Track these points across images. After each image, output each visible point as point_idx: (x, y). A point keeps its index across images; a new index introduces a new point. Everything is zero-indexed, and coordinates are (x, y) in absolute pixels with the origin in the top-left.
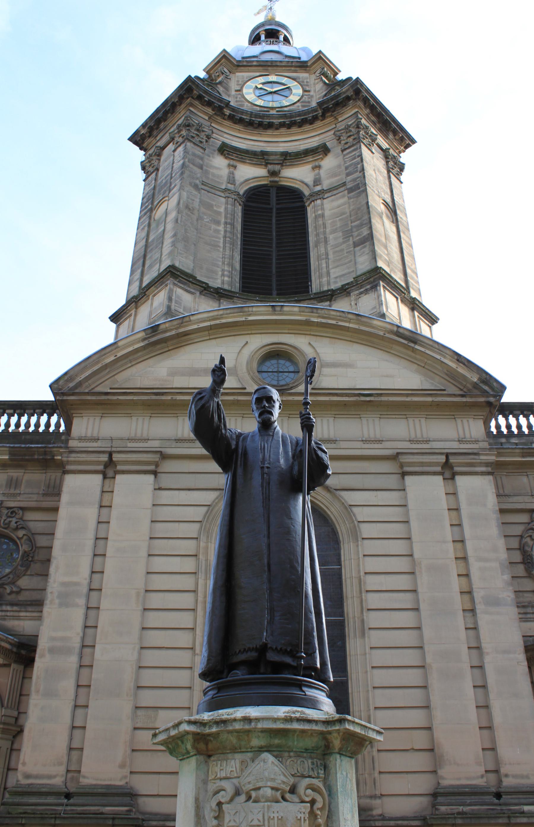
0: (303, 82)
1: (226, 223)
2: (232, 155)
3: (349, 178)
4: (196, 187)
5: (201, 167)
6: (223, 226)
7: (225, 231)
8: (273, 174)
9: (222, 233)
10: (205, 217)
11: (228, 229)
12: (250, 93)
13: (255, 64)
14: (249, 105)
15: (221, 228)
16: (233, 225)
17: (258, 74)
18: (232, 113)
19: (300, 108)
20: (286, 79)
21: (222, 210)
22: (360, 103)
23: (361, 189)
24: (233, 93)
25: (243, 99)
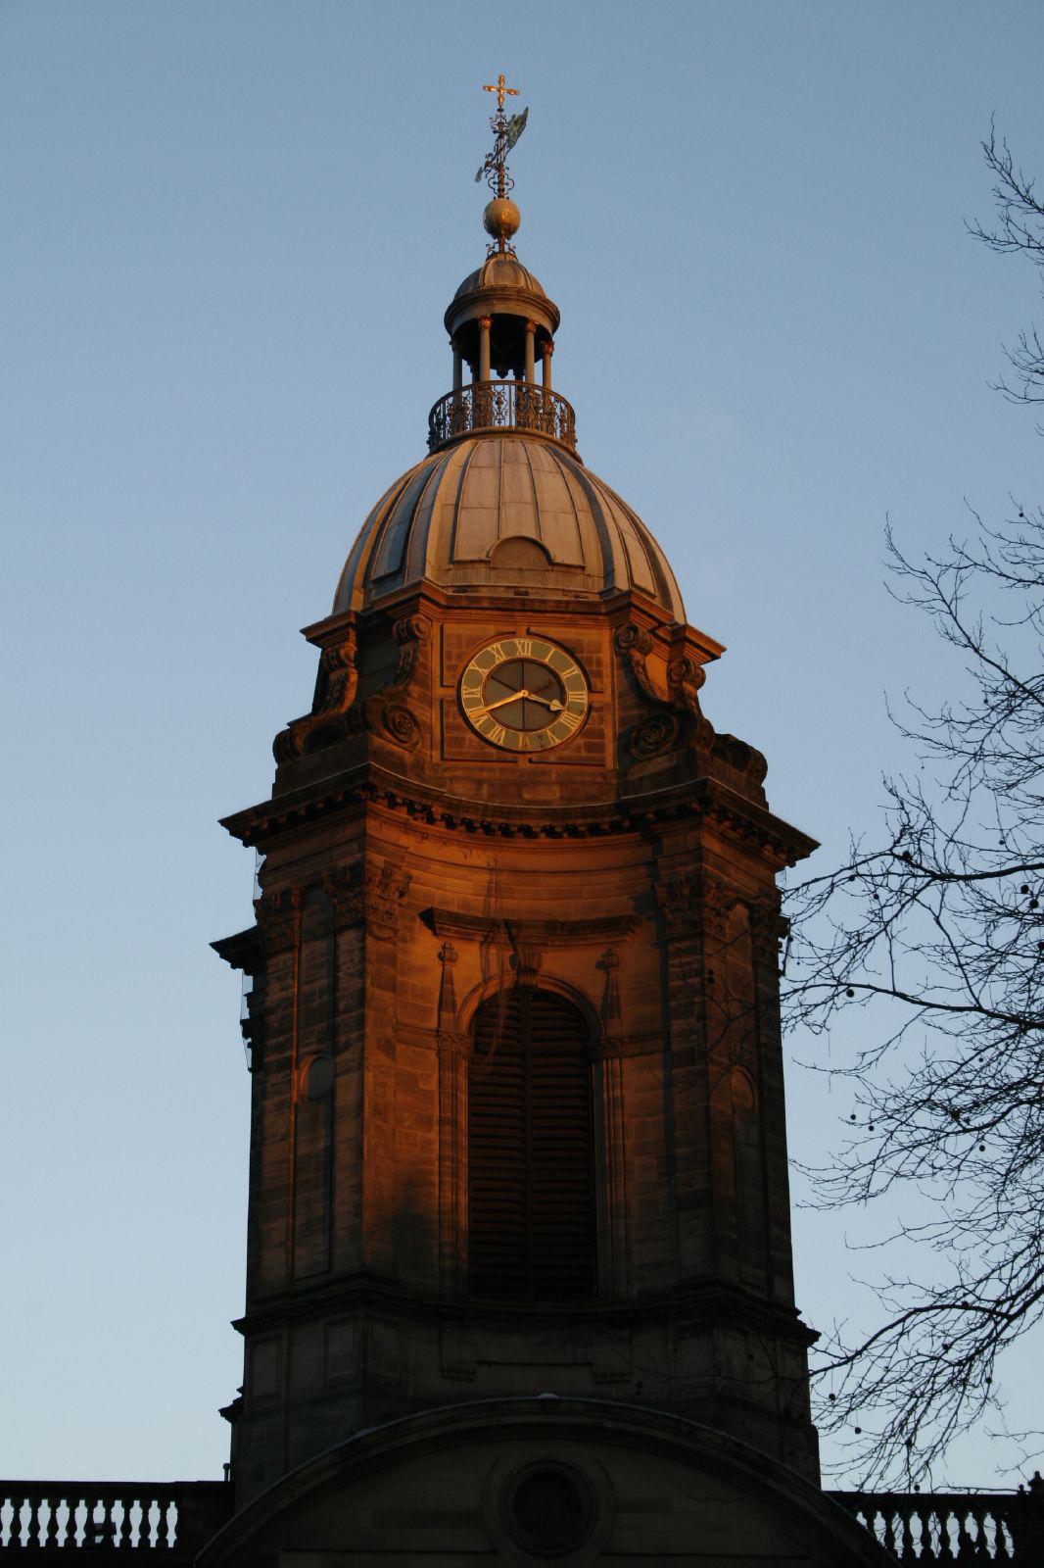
0: (590, 663)
1: (441, 1122)
2: (448, 931)
3: (677, 1025)
4: (388, 1048)
5: (393, 987)
6: (437, 1128)
7: (441, 1143)
8: (524, 969)
9: (436, 1146)
10: (406, 1115)
11: (448, 1138)
12: (474, 703)
13: (485, 604)
14: (476, 739)
15: (434, 1135)
16: (454, 1123)
17: (492, 629)
18: (448, 812)
19: (583, 753)
20: (553, 650)
21: (434, 1086)
22: (710, 820)
23: (697, 1067)
24: (439, 692)
25: (461, 721)
